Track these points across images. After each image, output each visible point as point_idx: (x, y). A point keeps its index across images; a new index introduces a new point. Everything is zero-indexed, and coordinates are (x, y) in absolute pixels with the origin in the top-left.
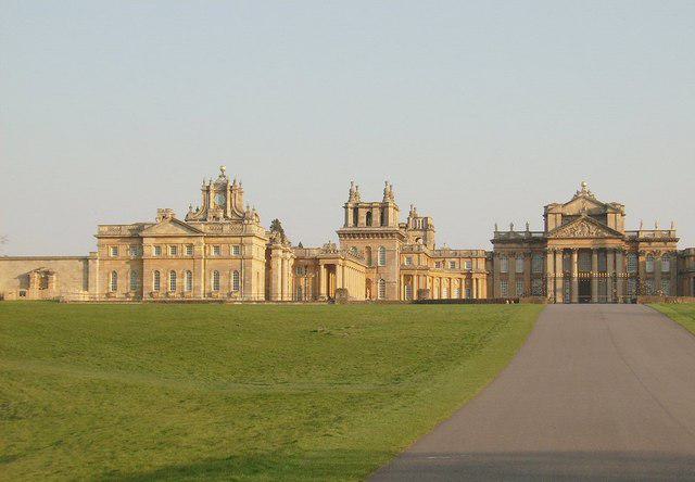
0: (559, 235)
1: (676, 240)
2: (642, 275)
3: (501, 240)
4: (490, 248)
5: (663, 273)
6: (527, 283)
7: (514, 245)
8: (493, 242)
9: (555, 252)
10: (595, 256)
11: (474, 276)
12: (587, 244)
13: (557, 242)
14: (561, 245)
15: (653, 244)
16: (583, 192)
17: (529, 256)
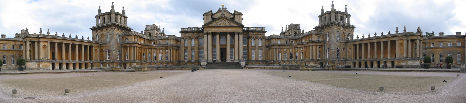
0: (212, 25)
1: (265, 32)
2: (250, 47)
3: (184, 32)
4: (179, 35)
5: (259, 47)
6: (196, 50)
7: (190, 34)
8: (181, 32)
9: (208, 34)
10: (228, 36)
11: (169, 48)
12: (223, 30)
13: (208, 29)
14: (210, 30)
15: (255, 33)
16: (223, 8)
17: (198, 38)
